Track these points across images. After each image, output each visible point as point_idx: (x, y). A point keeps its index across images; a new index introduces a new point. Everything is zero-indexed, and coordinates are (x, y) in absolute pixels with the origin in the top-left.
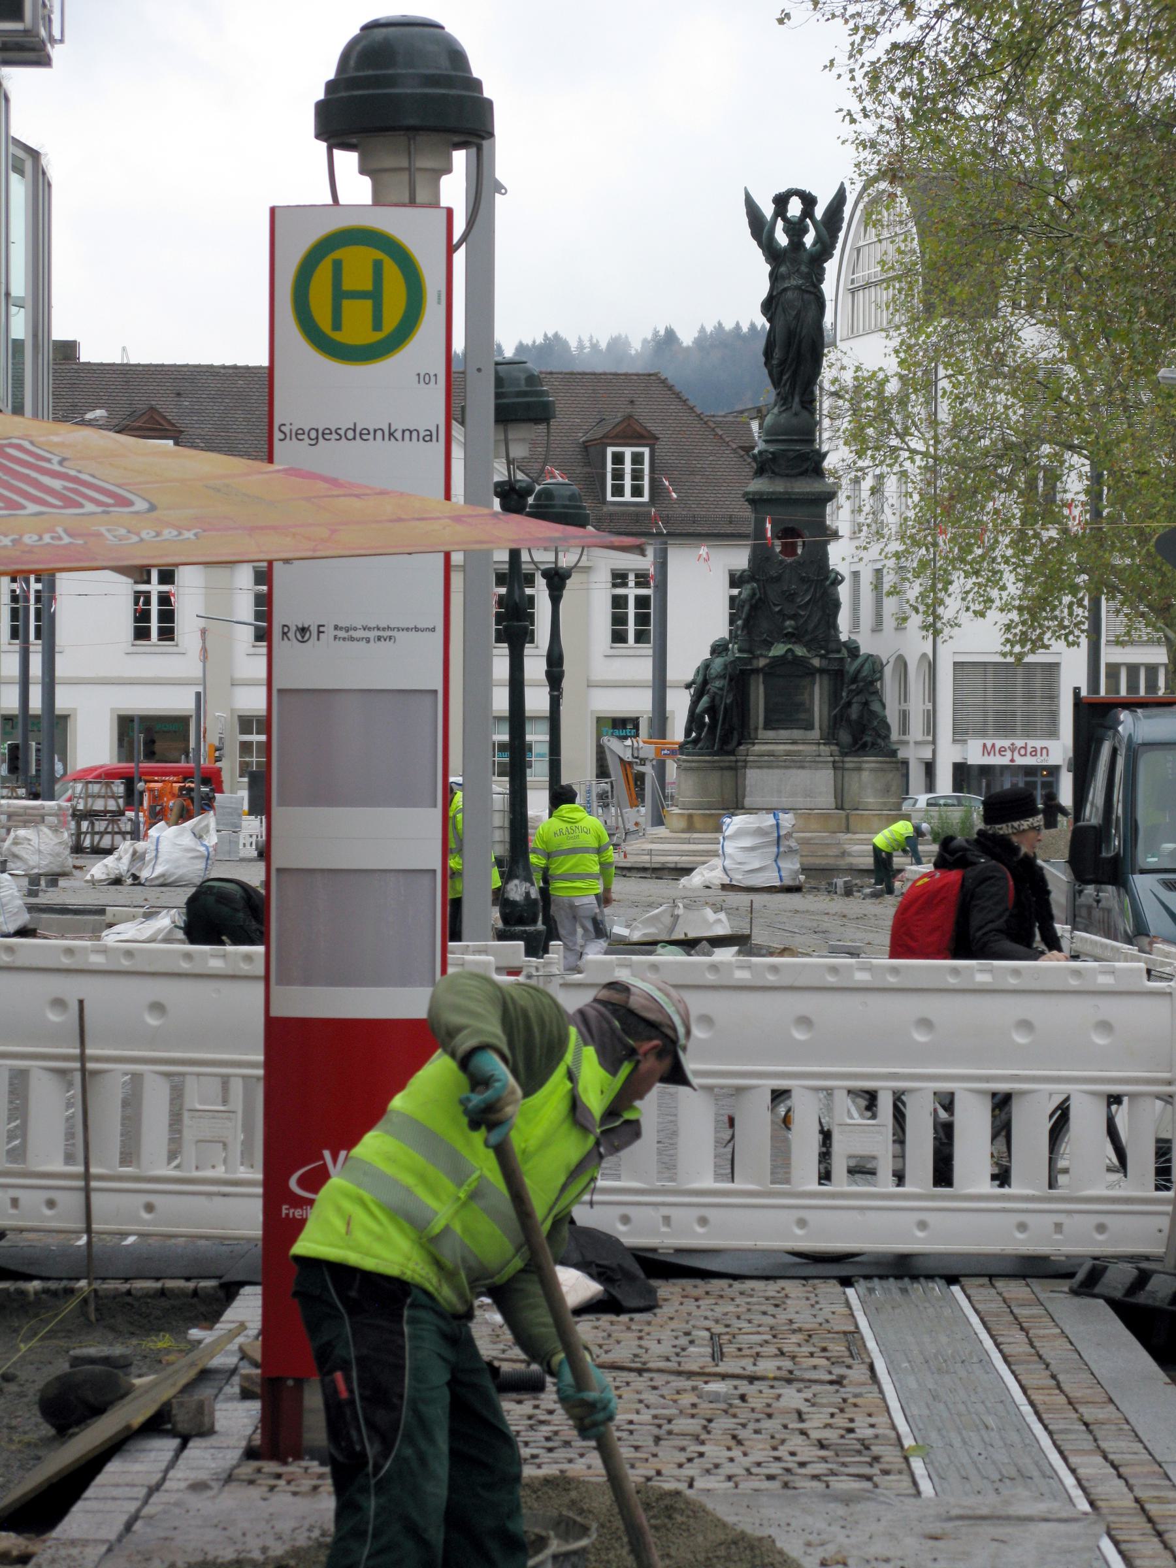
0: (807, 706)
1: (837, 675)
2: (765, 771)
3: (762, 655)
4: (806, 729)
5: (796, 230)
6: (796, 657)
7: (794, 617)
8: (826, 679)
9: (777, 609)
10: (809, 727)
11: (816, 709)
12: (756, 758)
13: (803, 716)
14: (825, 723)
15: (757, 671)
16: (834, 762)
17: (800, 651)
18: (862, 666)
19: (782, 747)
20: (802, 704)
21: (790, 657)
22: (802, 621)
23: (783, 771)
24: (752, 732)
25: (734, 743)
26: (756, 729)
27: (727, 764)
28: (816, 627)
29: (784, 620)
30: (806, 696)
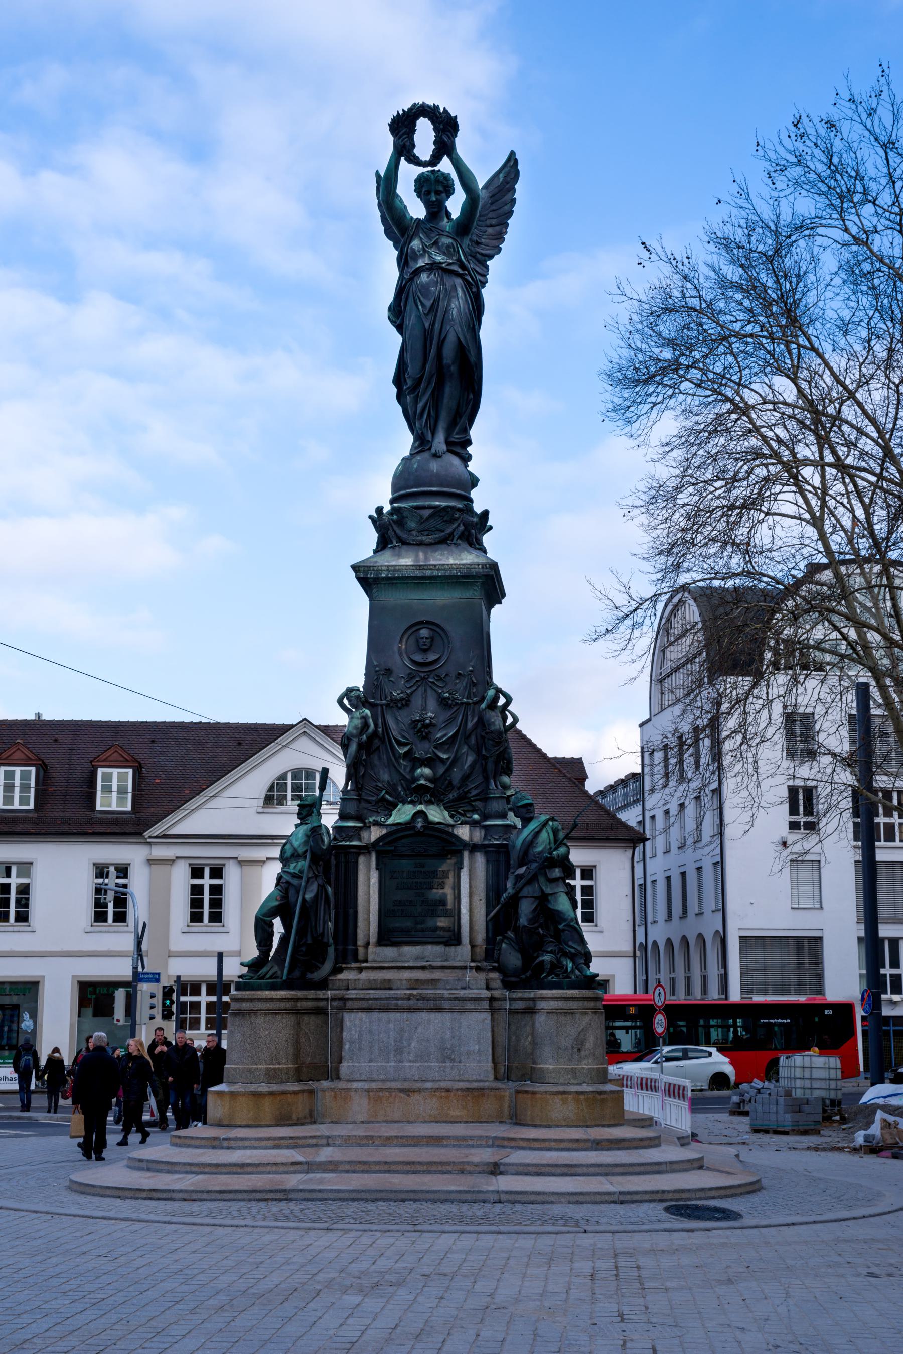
0: (450, 906)
1: (499, 857)
2: (376, 1015)
3: (376, 823)
4: (447, 944)
5: (433, 189)
6: (430, 825)
7: (429, 762)
8: (480, 860)
9: (402, 750)
10: (454, 939)
11: (464, 910)
12: (361, 993)
13: (442, 922)
14: (480, 937)
15: (366, 850)
16: (492, 999)
17: (436, 814)
18: (537, 834)
19: (407, 975)
20: (443, 902)
21: (419, 824)
22: (441, 770)
23: (405, 1015)
24: (361, 951)
25: (327, 967)
27: (310, 1004)
28: (466, 778)
29: (413, 769)
30: (448, 891)
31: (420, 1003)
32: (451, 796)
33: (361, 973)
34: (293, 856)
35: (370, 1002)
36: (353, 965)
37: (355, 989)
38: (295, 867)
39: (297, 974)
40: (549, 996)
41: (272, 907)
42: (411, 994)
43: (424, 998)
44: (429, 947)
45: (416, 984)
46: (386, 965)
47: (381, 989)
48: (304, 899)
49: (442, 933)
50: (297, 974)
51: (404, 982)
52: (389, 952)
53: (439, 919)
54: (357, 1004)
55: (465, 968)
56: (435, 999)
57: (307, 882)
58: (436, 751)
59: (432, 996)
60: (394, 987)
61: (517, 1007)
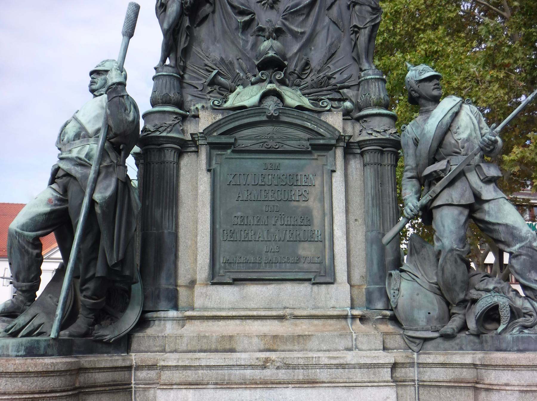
10: (324, 276)
12: (185, 359)
13: (306, 250)
14: (359, 272)
16: (394, 366)
19: (257, 327)
24: (183, 293)
25: (131, 317)
26: (192, 284)
29: (255, 46)
31: (282, 375)
32: (309, 79)
33: (183, 326)
34: (77, 136)
35: (200, 372)
36: (172, 314)
37: (176, 351)
38: (79, 152)
39: (81, 324)
40: (524, 363)
41: (40, 215)
42: (267, 360)
43: (287, 366)
44: (288, 287)
45: (273, 343)
46: (224, 314)
47: (216, 351)
48: (92, 202)
49: (306, 266)
50: (81, 324)
51: (255, 340)
52: (227, 296)
53: (302, 245)
54: (177, 376)
55: (345, 317)
56: (306, 367)
57: (98, 173)
58: (287, 23)
59: (301, 362)
60: (238, 348)
61: (433, 377)
